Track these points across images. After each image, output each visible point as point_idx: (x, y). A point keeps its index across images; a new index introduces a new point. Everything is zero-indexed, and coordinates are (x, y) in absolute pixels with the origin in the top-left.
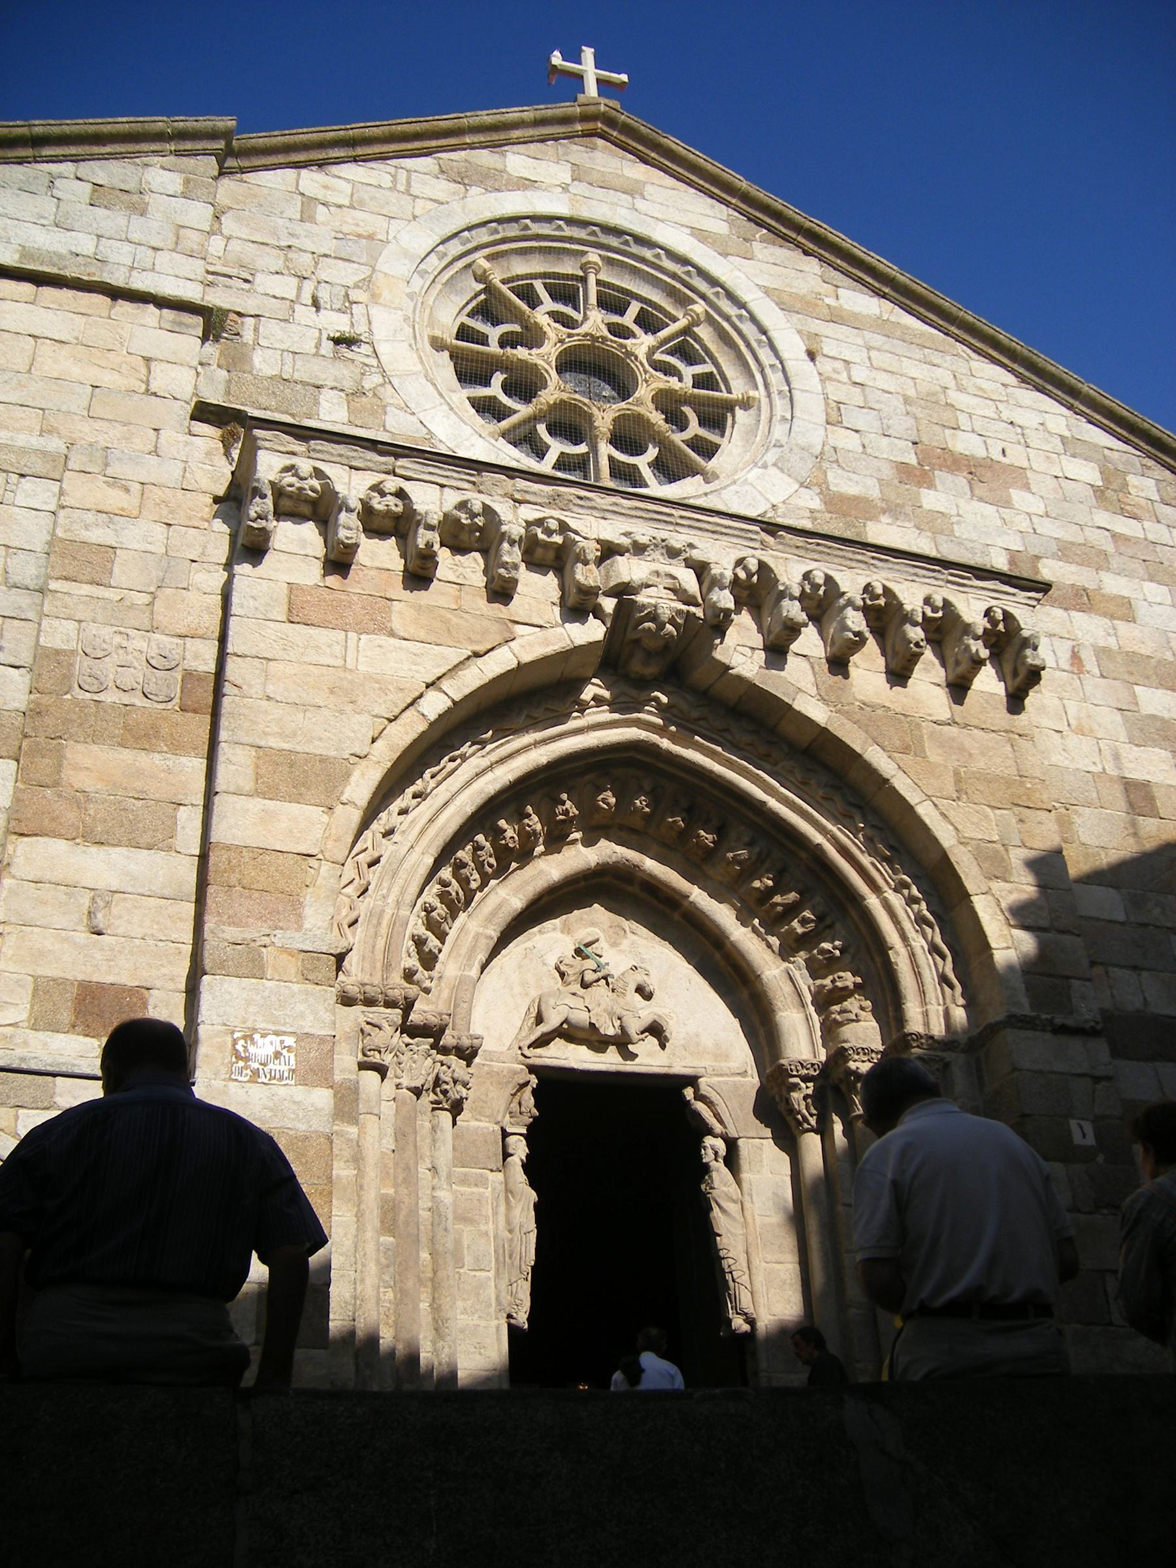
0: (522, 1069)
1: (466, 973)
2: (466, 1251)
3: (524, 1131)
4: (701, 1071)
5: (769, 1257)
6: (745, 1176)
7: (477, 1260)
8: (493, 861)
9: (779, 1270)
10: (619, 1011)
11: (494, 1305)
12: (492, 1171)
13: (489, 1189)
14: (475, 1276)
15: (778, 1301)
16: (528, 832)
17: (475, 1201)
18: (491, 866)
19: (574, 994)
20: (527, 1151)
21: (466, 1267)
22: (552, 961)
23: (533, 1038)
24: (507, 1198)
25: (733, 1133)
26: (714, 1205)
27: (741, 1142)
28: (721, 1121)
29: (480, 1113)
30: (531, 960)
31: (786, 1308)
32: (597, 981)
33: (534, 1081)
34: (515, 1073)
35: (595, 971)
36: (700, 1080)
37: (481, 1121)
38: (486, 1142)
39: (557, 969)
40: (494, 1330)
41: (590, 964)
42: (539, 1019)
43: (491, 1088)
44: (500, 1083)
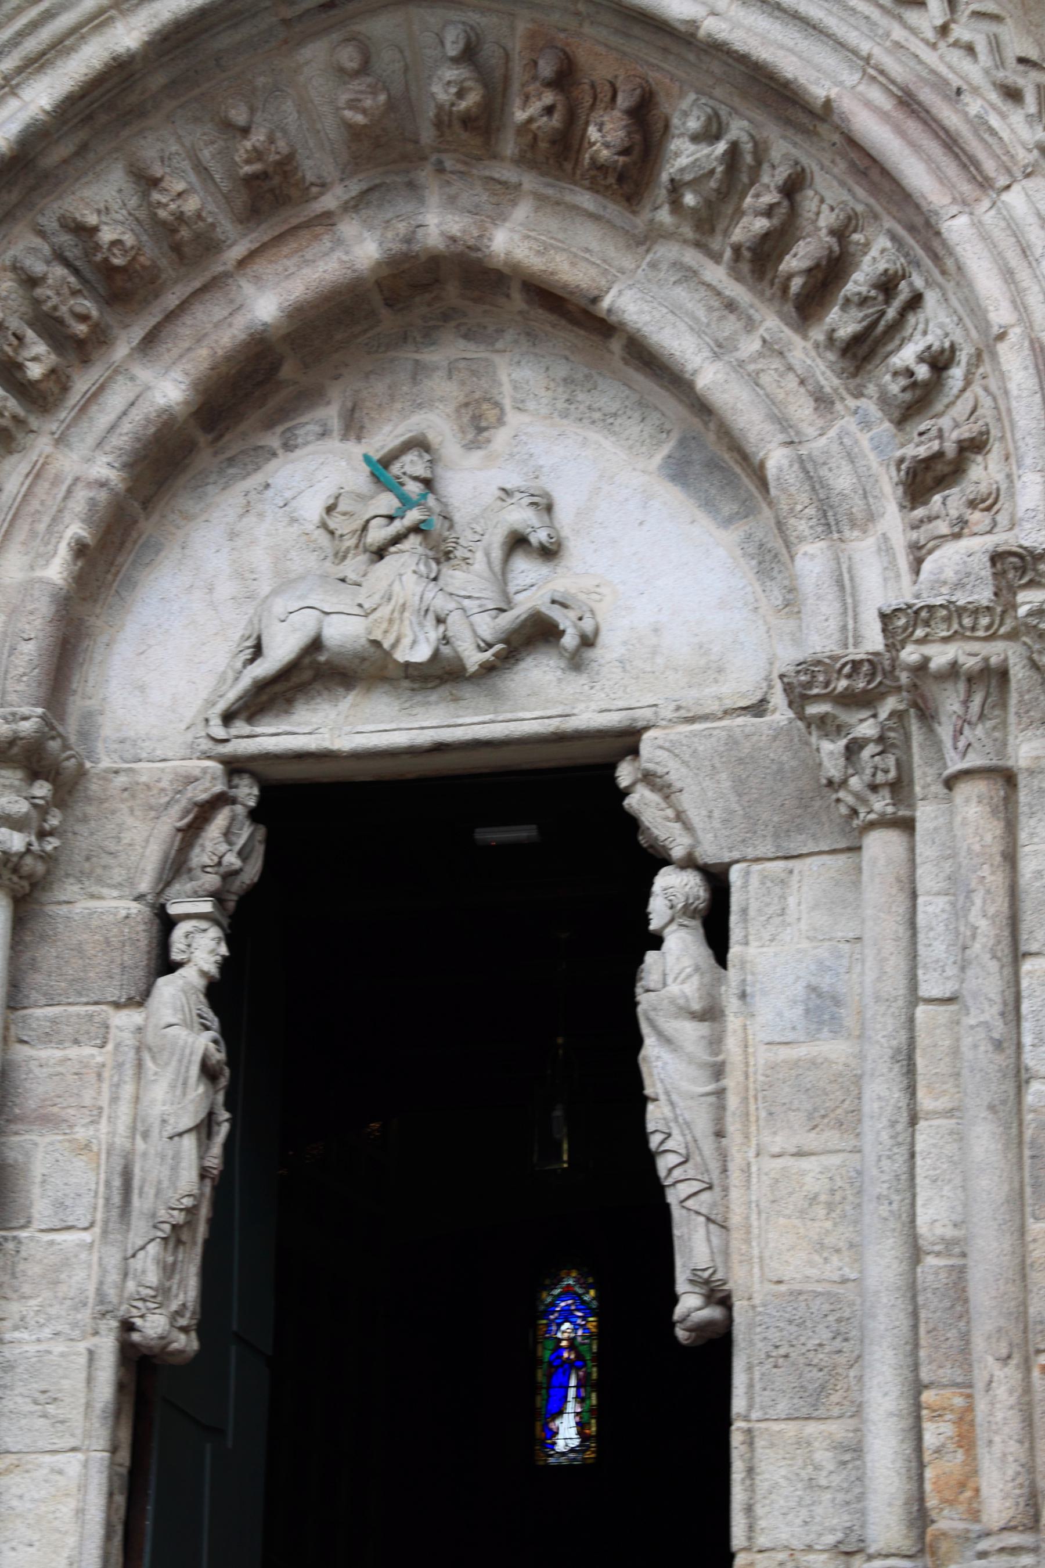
0: (205, 771)
1: (39, 573)
2: (36, 1190)
3: (206, 906)
4: (643, 716)
5: (777, 1143)
6: (734, 951)
7: (60, 1205)
8: (87, 305)
9: (803, 1173)
10: (441, 603)
11: (91, 1301)
12: (117, 1005)
13: (110, 1047)
14: (52, 1243)
15: (792, 1248)
16: (164, 223)
17: (70, 1078)
18: (84, 318)
19: (343, 580)
20: (224, 950)
21: (36, 1225)
22: (312, 508)
23: (232, 695)
24: (139, 1065)
25: (710, 852)
26: (645, 1029)
27: (735, 875)
28: (688, 827)
29: (100, 881)
30: (261, 515)
31: (811, 1264)
32: (397, 539)
33: (248, 793)
34: (190, 780)
35: (391, 518)
36: (647, 736)
37: (100, 898)
38: (107, 942)
39: (324, 525)
40: (83, 1360)
41: (387, 502)
42: (258, 651)
43: (130, 821)
44: (151, 808)
